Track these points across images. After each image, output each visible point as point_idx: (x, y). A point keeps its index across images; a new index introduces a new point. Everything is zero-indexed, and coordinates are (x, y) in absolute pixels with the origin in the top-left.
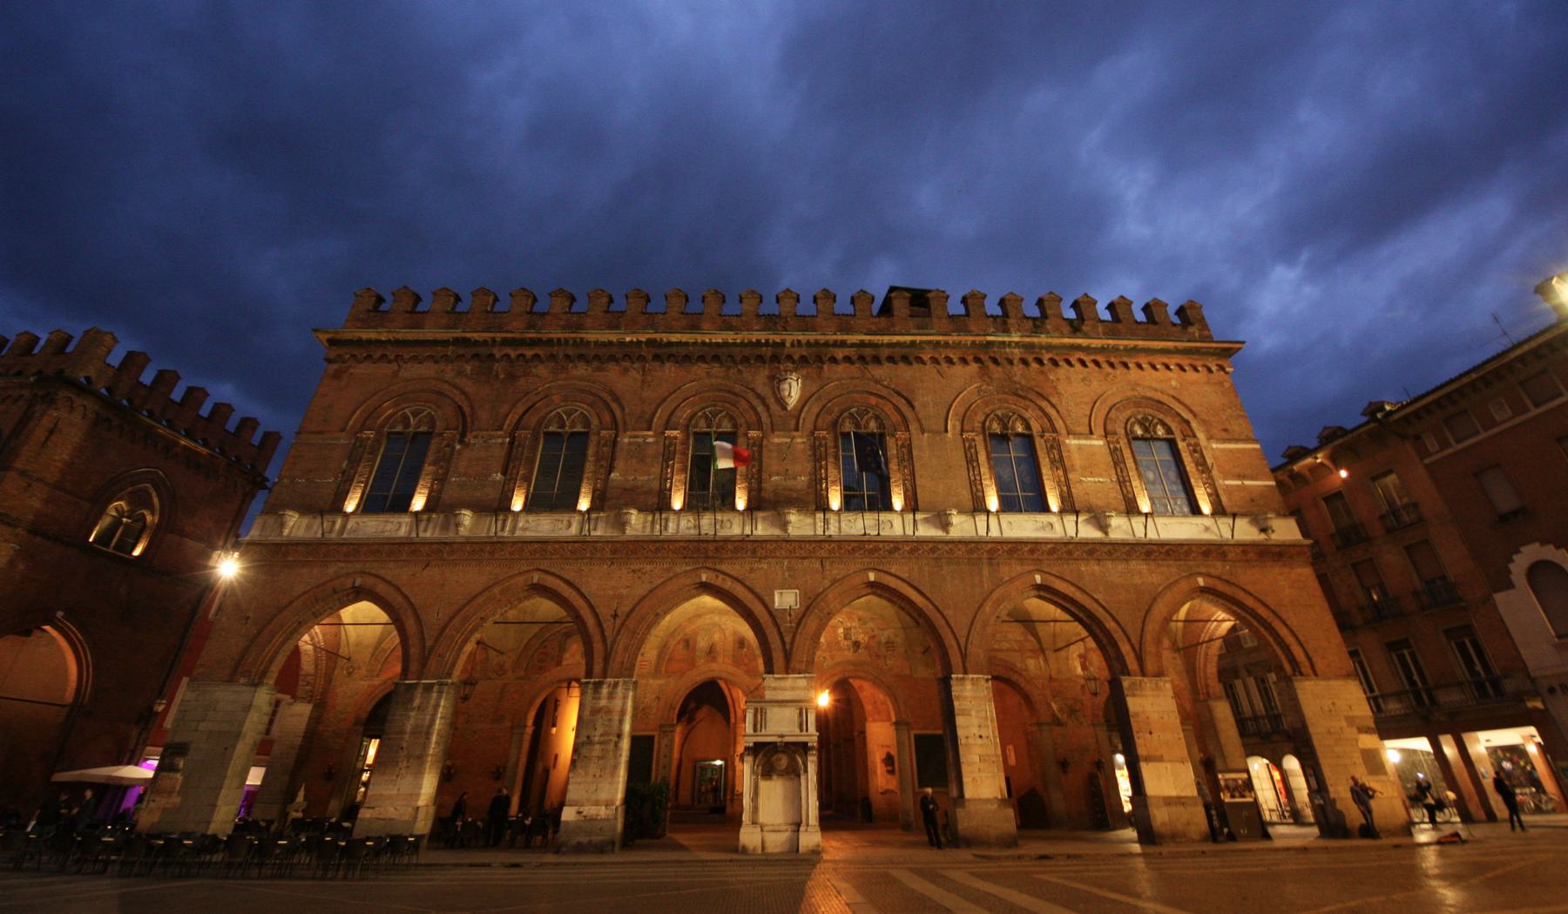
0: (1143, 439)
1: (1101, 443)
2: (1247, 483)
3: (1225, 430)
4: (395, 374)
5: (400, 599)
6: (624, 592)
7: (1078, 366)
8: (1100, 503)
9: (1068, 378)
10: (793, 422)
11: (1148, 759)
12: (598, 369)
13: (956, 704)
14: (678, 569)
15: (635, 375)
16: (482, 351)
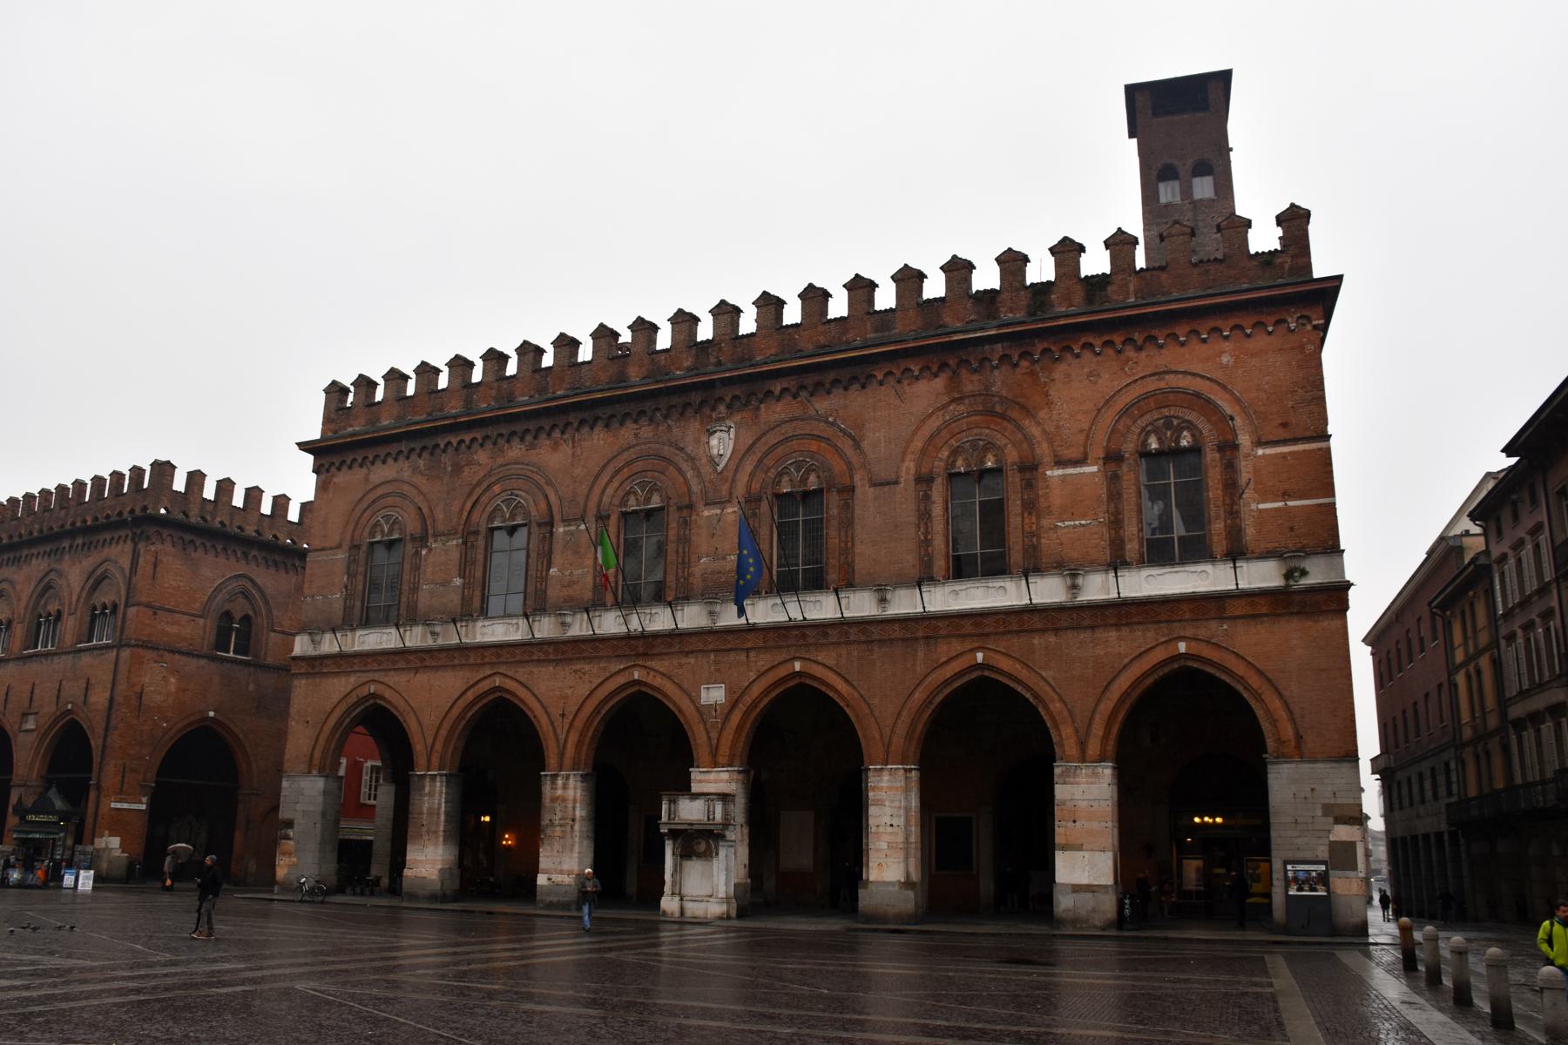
0: (1159, 454)
1: (1094, 469)
2: (1291, 503)
3: (1284, 425)
4: (367, 480)
5: (402, 703)
6: (569, 691)
7: (1087, 355)
8: (1075, 555)
9: (1069, 376)
10: (725, 488)
11: (1064, 848)
12: (532, 447)
13: (871, 794)
14: (616, 666)
15: (566, 449)
16: (430, 443)
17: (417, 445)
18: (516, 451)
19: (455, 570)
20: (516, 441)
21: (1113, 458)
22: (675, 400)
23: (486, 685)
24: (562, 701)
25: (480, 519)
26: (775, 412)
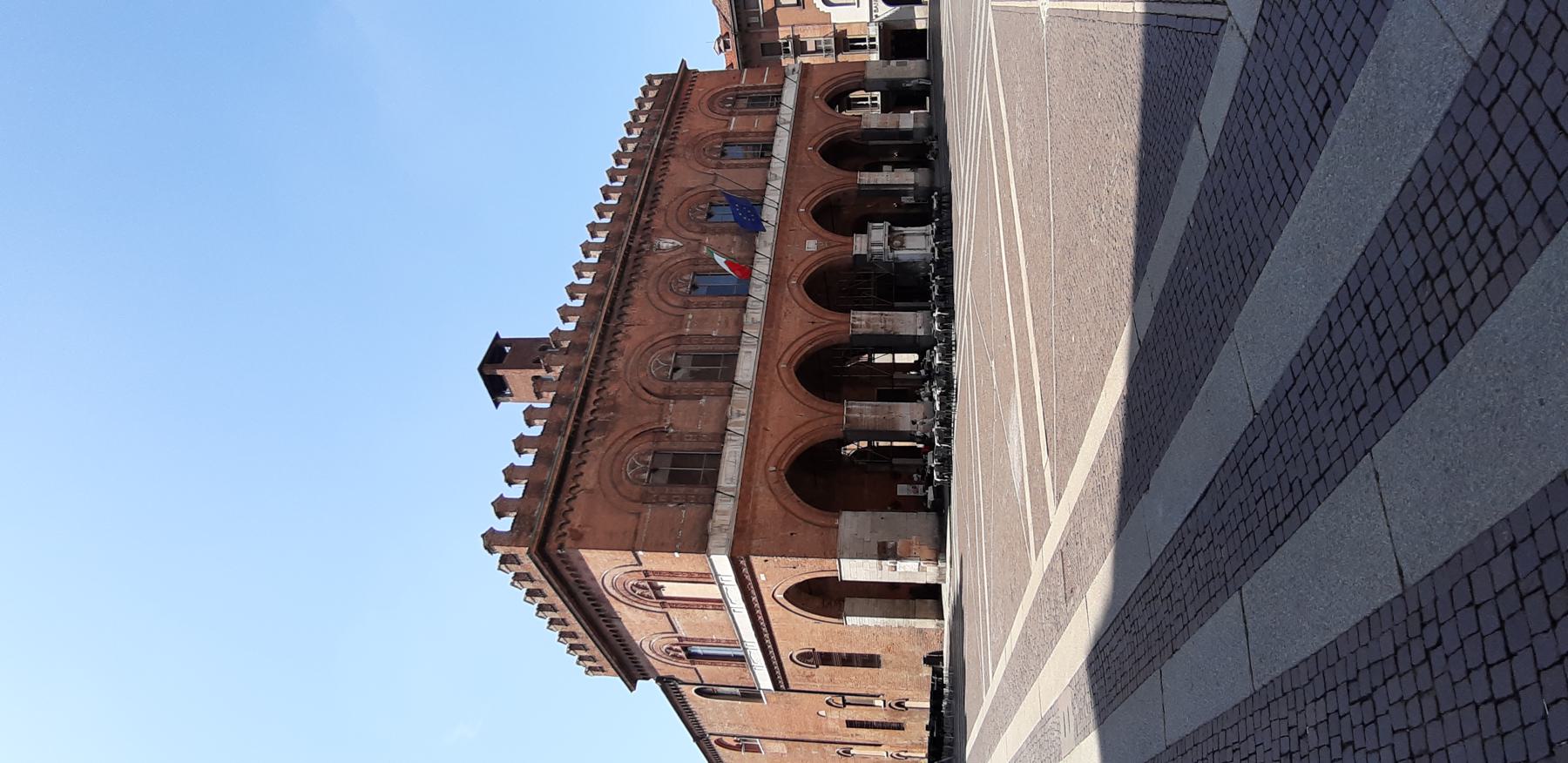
4: (591, 491)
10: (694, 244)
12: (621, 353)
17: (581, 437)
18: (619, 363)
19: (693, 403)
20: (613, 364)
21: (730, 114)
22: (630, 266)
23: (784, 375)
24: (803, 324)
25: (658, 387)
26: (658, 222)
